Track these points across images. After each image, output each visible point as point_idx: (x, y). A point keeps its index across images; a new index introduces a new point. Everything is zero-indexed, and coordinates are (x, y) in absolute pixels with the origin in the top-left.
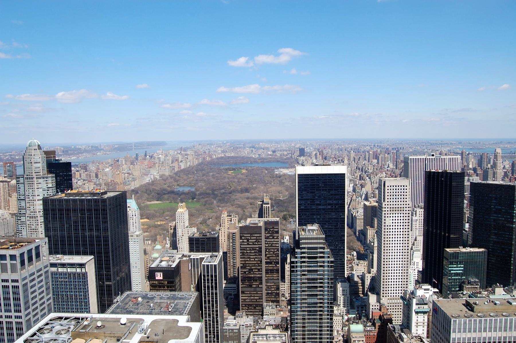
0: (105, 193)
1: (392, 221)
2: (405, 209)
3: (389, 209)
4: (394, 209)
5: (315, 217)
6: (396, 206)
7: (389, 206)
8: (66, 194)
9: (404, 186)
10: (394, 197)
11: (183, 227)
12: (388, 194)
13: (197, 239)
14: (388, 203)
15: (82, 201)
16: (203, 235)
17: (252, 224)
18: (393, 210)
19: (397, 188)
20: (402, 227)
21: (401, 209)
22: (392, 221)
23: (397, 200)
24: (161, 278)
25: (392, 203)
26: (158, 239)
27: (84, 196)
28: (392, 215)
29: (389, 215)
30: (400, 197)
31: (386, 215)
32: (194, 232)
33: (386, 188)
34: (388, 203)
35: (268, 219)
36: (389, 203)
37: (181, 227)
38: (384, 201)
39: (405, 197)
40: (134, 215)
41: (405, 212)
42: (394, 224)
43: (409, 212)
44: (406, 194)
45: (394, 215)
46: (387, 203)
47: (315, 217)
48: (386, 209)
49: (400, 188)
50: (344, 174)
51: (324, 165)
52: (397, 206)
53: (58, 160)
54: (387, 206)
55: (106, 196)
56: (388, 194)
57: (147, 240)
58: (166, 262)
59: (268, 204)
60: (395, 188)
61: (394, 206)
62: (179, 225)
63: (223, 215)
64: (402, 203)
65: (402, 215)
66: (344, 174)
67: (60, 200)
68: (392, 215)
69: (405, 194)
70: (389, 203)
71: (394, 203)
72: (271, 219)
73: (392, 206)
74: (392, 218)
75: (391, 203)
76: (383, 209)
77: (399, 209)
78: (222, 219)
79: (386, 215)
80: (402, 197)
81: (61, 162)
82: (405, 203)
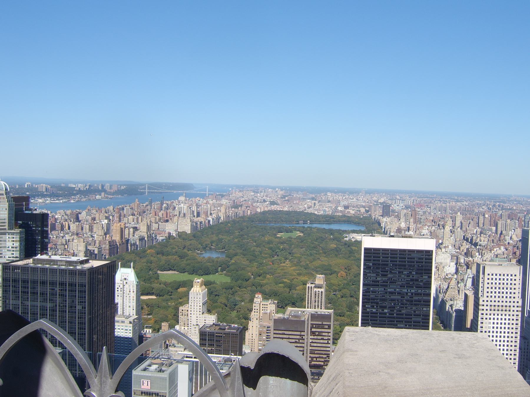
0: (87, 261)
1: (492, 325)
2: (512, 309)
3: (488, 308)
4: (496, 308)
5: (386, 311)
6: (498, 304)
7: (489, 303)
8: (34, 260)
9: (511, 275)
10: (497, 290)
11: (198, 313)
12: (488, 286)
13: (211, 334)
14: (487, 299)
15: (53, 271)
16: (220, 329)
17: (292, 316)
18: (495, 308)
19: (502, 277)
20: (506, 335)
21: (506, 309)
22: (492, 325)
23: (501, 295)
24: (149, 387)
25: (493, 299)
26: (163, 328)
27: (57, 265)
28: (492, 317)
29: (488, 317)
30: (505, 291)
31: (485, 316)
32: (211, 319)
33: (486, 277)
34: (487, 299)
35: (316, 310)
36: (489, 299)
37: (195, 312)
38: (482, 296)
39: (513, 291)
40: (132, 291)
41: (511, 313)
42: (495, 330)
43: (517, 313)
44: (515, 287)
45: (496, 317)
46: (485, 299)
47: (386, 311)
48: (485, 308)
49: (506, 277)
50: (432, 251)
51: (402, 237)
52: (500, 304)
53: (31, 210)
54: (485, 303)
55: (87, 266)
56: (488, 286)
57: (147, 327)
58: (157, 366)
59: (321, 288)
60: (498, 277)
61: (497, 304)
62: (192, 310)
63: (255, 299)
64: (508, 300)
65: (507, 317)
66: (432, 251)
67: (25, 268)
68: (492, 317)
69: (513, 286)
70: (489, 299)
71: (497, 299)
72: (324, 311)
73: (493, 303)
74: (492, 321)
75: (491, 299)
76: (480, 307)
77: (504, 308)
78: (254, 305)
79: (485, 316)
80: (509, 291)
81: (35, 212)
82: (512, 300)
